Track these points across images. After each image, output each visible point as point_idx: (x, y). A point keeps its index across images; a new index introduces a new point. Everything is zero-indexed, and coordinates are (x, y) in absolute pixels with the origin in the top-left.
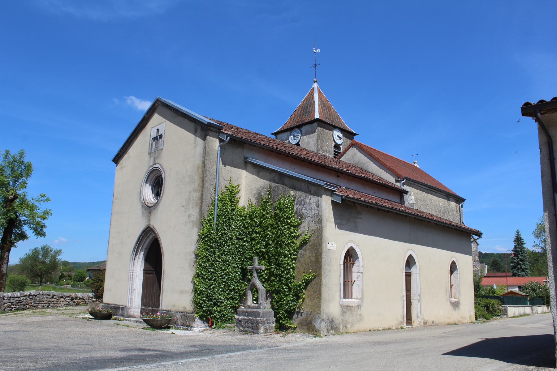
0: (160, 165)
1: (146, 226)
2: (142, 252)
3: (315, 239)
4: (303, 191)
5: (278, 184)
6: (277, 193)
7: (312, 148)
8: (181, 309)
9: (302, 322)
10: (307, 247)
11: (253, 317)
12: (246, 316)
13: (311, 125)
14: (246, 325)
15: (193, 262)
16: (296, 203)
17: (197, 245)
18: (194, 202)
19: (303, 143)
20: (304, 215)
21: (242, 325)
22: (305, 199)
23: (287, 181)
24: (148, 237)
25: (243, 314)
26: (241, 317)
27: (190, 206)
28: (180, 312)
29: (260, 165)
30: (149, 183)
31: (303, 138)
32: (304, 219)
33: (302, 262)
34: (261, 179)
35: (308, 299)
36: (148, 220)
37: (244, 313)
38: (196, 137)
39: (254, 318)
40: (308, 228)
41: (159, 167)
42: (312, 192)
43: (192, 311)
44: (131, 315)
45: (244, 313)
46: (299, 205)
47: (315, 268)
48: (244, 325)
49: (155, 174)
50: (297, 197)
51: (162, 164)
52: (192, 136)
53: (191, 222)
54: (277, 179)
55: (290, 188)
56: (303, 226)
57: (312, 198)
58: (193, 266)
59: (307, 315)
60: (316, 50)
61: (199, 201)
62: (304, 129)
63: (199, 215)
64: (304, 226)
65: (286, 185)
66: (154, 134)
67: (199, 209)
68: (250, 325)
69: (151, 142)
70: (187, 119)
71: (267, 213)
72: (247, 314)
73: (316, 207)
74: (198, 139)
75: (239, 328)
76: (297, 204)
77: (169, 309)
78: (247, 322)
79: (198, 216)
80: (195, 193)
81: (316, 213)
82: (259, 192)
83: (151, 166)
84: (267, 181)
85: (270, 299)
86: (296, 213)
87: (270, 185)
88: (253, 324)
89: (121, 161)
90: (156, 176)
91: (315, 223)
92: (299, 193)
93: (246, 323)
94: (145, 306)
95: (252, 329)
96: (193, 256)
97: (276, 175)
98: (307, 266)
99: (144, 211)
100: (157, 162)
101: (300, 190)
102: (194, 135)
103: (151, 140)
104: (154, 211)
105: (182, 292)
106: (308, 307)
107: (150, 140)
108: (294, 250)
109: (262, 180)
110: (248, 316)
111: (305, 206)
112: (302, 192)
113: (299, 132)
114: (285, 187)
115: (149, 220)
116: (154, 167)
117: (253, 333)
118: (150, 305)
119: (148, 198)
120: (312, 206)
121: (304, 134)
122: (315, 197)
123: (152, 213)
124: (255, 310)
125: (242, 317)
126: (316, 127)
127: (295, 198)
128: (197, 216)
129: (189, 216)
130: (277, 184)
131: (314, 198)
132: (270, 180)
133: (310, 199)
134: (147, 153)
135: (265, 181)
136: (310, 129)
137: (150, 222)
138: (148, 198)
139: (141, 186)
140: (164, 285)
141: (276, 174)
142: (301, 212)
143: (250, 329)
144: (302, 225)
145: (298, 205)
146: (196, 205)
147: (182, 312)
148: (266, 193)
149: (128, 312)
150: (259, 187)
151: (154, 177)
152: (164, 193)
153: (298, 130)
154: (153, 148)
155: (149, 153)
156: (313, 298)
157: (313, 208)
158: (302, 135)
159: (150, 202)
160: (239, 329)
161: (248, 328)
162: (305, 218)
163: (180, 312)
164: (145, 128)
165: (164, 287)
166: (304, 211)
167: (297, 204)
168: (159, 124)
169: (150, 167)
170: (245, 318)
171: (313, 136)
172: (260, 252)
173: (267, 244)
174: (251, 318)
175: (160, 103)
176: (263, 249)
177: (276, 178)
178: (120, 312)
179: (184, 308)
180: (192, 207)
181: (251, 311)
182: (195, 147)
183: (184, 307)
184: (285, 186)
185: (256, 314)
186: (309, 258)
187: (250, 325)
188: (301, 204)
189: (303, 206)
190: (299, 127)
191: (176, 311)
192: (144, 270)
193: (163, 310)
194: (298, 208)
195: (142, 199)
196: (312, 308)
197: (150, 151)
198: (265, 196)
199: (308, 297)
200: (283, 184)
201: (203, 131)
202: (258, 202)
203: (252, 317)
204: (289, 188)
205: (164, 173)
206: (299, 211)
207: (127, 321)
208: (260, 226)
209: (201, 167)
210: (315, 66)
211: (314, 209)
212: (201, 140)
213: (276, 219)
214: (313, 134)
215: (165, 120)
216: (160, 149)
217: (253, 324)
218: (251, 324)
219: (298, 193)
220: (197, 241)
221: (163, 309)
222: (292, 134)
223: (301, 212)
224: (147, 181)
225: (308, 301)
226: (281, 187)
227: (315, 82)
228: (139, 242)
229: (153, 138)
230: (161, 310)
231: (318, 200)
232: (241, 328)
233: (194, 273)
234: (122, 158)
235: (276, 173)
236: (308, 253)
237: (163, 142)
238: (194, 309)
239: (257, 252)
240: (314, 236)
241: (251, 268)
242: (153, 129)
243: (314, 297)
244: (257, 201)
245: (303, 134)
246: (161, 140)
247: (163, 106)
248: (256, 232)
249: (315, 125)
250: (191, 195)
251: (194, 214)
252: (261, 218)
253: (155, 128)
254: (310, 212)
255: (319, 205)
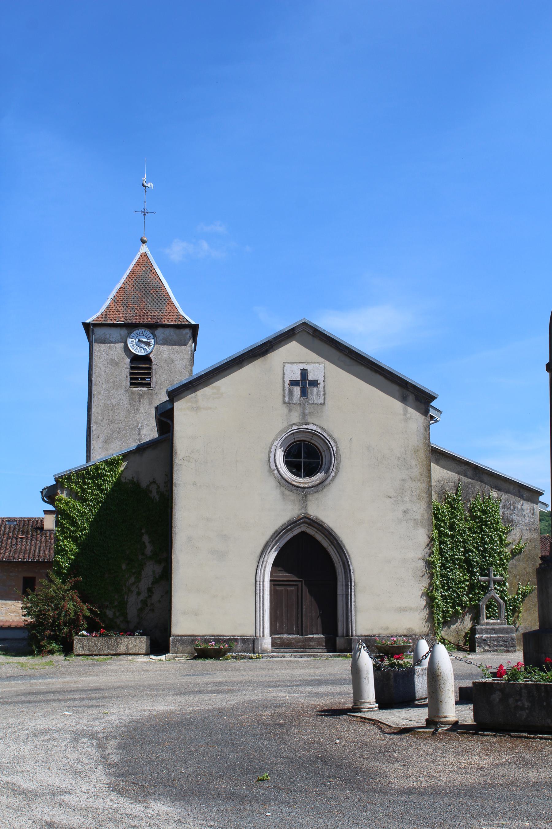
0: (321, 428)
1: (296, 515)
2: (275, 552)
3: (531, 549)
4: (511, 494)
5: (473, 481)
6: (471, 491)
7: (179, 371)
8: (405, 632)
9: (520, 638)
10: (520, 557)
11: (504, 634)
12: (492, 634)
13: (178, 331)
14: (495, 643)
15: (422, 572)
16: (502, 507)
17: (427, 550)
18: (413, 494)
19: (159, 357)
20: (514, 522)
21: (488, 645)
22: (515, 504)
23: (486, 478)
24: (292, 532)
25: (487, 632)
26: (485, 636)
27: (407, 499)
28: (401, 636)
29: (444, 453)
30: (283, 448)
31: (158, 350)
32: (514, 526)
33: (515, 573)
34: (442, 470)
35: (526, 613)
36: (300, 507)
37: (487, 631)
38: (404, 405)
39: (507, 635)
40: (521, 535)
41: (319, 431)
42: (525, 498)
43: (426, 633)
44: (265, 649)
45: (489, 631)
46: (506, 509)
47: (533, 580)
48: (491, 644)
49: (295, 437)
50: (503, 500)
51: (325, 427)
52: (398, 405)
53: (411, 519)
54: (470, 473)
55: (491, 488)
56: (514, 533)
57: (524, 504)
58: (423, 576)
59: (525, 630)
60: (147, 184)
61: (424, 495)
62: (159, 332)
63: (428, 513)
64: (516, 534)
65: (485, 483)
66: (298, 377)
67: (426, 505)
68: (501, 643)
69: (287, 386)
70: (380, 374)
71: (461, 514)
72: (493, 631)
73: (530, 514)
74: (411, 410)
75: (483, 648)
76: (504, 507)
77: (375, 632)
78: (497, 640)
79: (426, 514)
80: (414, 482)
81: (531, 521)
82: (442, 485)
83: (295, 424)
84: (453, 474)
85: (470, 614)
86: (503, 519)
87: (459, 479)
88: (505, 641)
89: (193, 395)
90: (296, 440)
91: (530, 532)
92: (506, 496)
93: (494, 641)
94: (282, 634)
95: (506, 647)
96: (421, 564)
97: (467, 468)
98: (522, 578)
99: (287, 492)
100: (310, 420)
101: (507, 492)
102: (401, 402)
103: (287, 381)
104: (316, 495)
105: (402, 610)
106: (526, 622)
107: (284, 382)
108: (507, 560)
109: (445, 470)
110: (495, 633)
111: (515, 512)
112: (510, 495)
113: (151, 335)
114: (484, 485)
115: (305, 507)
116: (301, 427)
117: (508, 651)
118: (295, 633)
119: (284, 472)
120: (524, 513)
121: (161, 342)
122: (530, 503)
123: (310, 498)
124: (501, 626)
125: (486, 635)
126: (188, 338)
127: (501, 500)
128: (423, 513)
129: (405, 512)
130: (470, 480)
131: (527, 504)
132: (458, 473)
133: (522, 505)
134: (281, 400)
135: (450, 473)
136: (175, 338)
137: (306, 510)
138: (284, 472)
139: (270, 452)
140: (357, 600)
141: (469, 468)
142: (510, 518)
143: (503, 648)
144: (512, 533)
145: (505, 509)
146: (420, 499)
147: (404, 636)
148: (453, 488)
149: (261, 645)
150: (441, 479)
151: (294, 441)
152: (340, 471)
153: (147, 332)
154: (295, 398)
155: (284, 403)
156: (532, 612)
157: (527, 515)
158: (156, 343)
159: (290, 478)
160: (484, 649)
161: (499, 646)
162: (516, 526)
163: (401, 636)
164: (265, 357)
165: (357, 605)
166: (515, 517)
167: (504, 507)
168: (307, 363)
169: (292, 425)
170: (492, 635)
171: (181, 352)
172: (457, 559)
173: (467, 551)
174: (501, 635)
175: (311, 332)
176: (461, 555)
177: (468, 473)
178: (240, 646)
179: (409, 629)
180: (410, 500)
181: (500, 628)
182: (406, 420)
183: (409, 629)
184: (484, 485)
185: (509, 630)
186: (525, 569)
187: (501, 643)
188: (509, 509)
189: (513, 511)
190: (153, 327)
191: (392, 634)
192: (271, 581)
193: (357, 636)
194: (506, 513)
195: (276, 472)
196: (532, 623)
197: (287, 399)
198: (451, 492)
199: (526, 611)
200: (481, 482)
201: (421, 402)
202: (440, 497)
203: (502, 634)
204: (489, 488)
205: (336, 442)
206: (507, 516)
207: (272, 657)
208: (452, 527)
209: (423, 451)
210: (145, 213)
211: (528, 517)
212: (418, 414)
213: (477, 523)
214: (183, 347)
215: (322, 360)
216: (315, 402)
217: (505, 641)
218: (503, 641)
219: (504, 496)
220: (428, 545)
221: (359, 634)
222: (133, 334)
223: (510, 518)
224: (281, 445)
225: (526, 615)
226: (478, 485)
227: (144, 242)
228: (277, 539)
229: (290, 380)
230: (356, 636)
231: (534, 508)
232: (487, 648)
233: (425, 583)
234: (196, 391)
235: (468, 466)
236: (522, 564)
237: (322, 393)
238: (430, 630)
239: (451, 559)
240: (529, 546)
241: (487, 579)
242: (287, 366)
243: (534, 611)
244: (438, 496)
245: (159, 342)
246: (315, 389)
247: (314, 336)
248: (446, 535)
249: (187, 334)
250: (406, 485)
251: (415, 509)
252: (450, 519)
253: (295, 366)
254: (523, 520)
255: (534, 513)
